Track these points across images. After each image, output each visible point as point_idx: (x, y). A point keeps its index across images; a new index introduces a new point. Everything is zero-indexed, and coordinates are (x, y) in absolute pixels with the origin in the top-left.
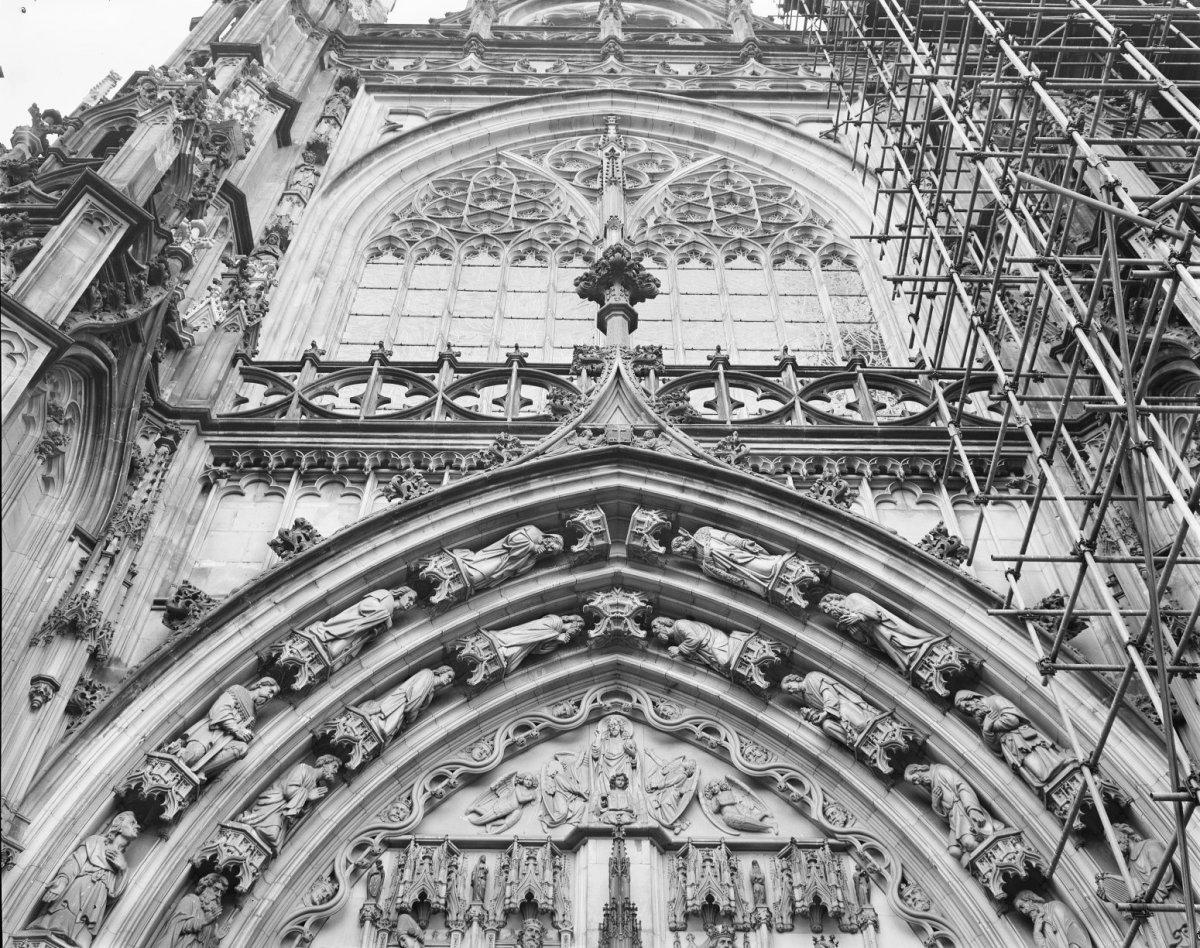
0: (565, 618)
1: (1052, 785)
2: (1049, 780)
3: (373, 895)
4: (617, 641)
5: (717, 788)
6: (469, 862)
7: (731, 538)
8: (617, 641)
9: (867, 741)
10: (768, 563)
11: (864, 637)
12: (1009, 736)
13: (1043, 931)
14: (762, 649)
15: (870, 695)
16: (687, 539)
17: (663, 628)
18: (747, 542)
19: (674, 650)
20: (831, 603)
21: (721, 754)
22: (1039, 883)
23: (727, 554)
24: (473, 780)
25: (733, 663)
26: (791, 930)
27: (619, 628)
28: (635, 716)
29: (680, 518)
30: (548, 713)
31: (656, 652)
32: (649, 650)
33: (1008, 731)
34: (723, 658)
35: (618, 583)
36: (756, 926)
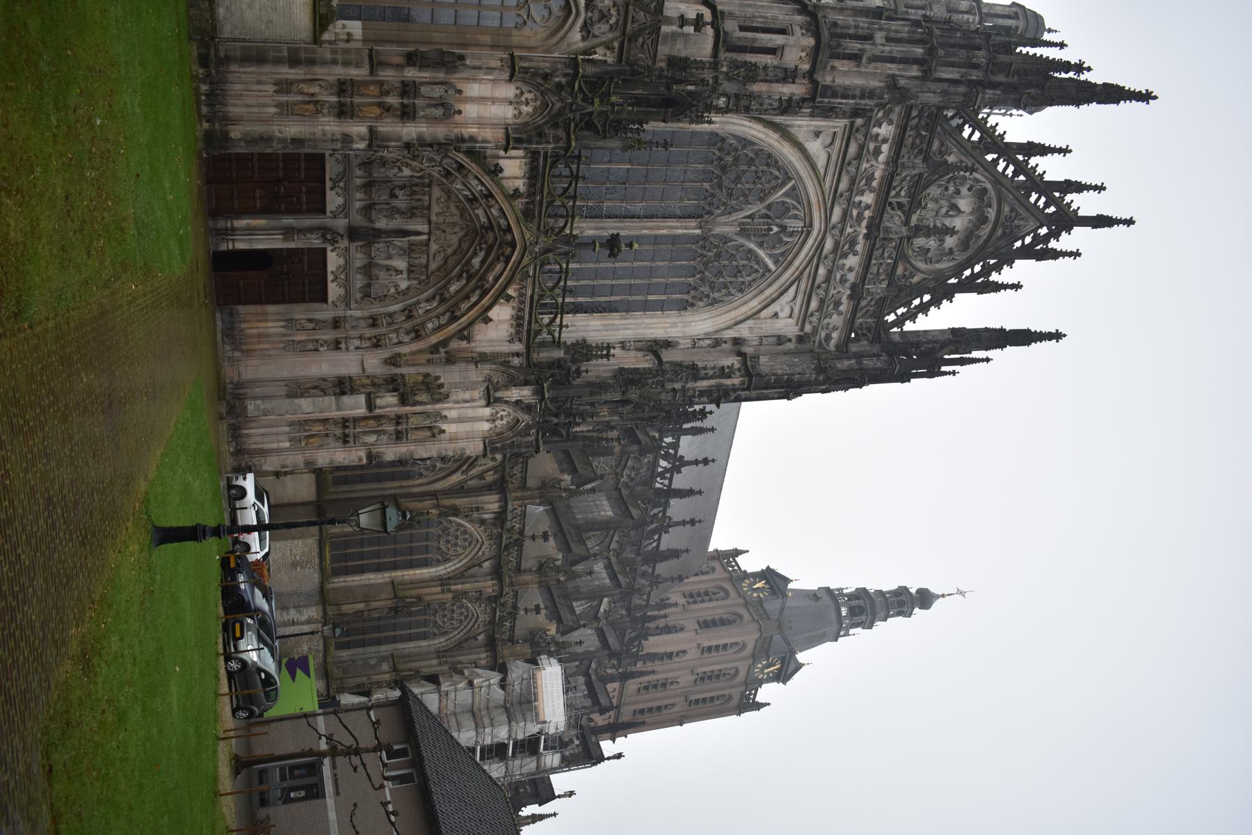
3: (418, 177)
4: (483, 236)
6: (426, 198)
8: (483, 236)
10: (491, 279)
15: (457, 292)
21: (454, 254)
24: (449, 197)
28: (466, 235)
30: (467, 214)
34: (473, 261)
36: (409, 258)
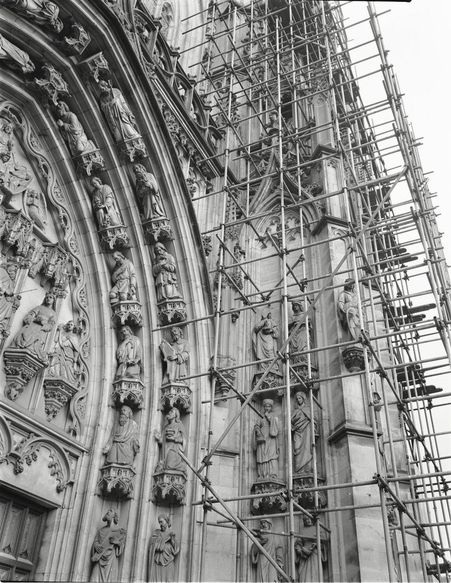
0: (30, 61)
1: (170, 301)
2: (170, 298)
4: (41, 95)
5: (36, 195)
7: (126, 106)
9: (113, 231)
11: (141, 194)
12: (167, 273)
13: (127, 344)
14: (99, 159)
16: (109, 87)
17: (64, 109)
18: (131, 115)
19: (61, 123)
20: (141, 169)
22: (135, 327)
23: (121, 111)
25: (84, 153)
26: (33, 278)
27: (48, 90)
29: (113, 75)
31: (50, 115)
32: (48, 111)
33: (168, 271)
35: (61, 69)
